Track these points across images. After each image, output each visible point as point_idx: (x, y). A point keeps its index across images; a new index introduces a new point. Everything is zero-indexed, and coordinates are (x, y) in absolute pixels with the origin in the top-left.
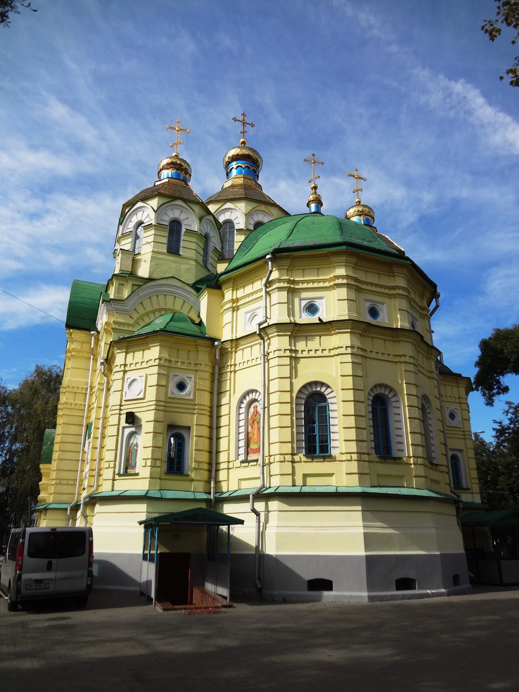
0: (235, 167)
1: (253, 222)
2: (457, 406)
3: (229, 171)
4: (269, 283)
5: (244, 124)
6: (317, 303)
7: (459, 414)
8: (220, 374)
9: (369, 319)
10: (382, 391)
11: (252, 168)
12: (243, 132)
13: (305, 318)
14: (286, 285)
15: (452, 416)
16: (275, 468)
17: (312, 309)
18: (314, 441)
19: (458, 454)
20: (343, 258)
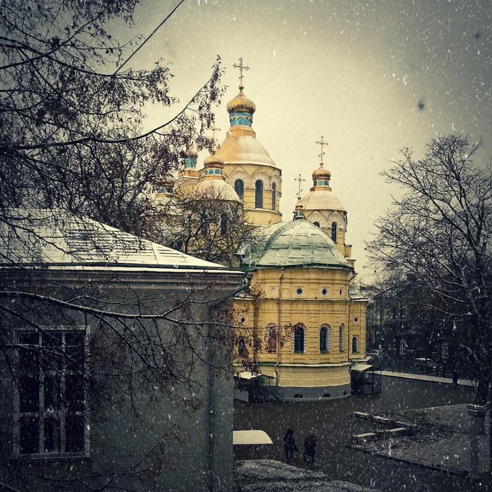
0: (237, 117)
1: (255, 182)
2: (359, 314)
3: (232, 119)
4: (281, 279)
5: (241, 67)
6: (303, 289)
7: (359, 318)
8: (258, 313)
9: (321, 297)
10: (324, 326)
11: (249, 118)
12: (241, 77)
13: (295, 296)
14: (288, 281)
15: (356, 320)
16: (283, 356)
17: (300, 291)
18: (299, 347)
19: (357, 337)
20: (314, 270)
